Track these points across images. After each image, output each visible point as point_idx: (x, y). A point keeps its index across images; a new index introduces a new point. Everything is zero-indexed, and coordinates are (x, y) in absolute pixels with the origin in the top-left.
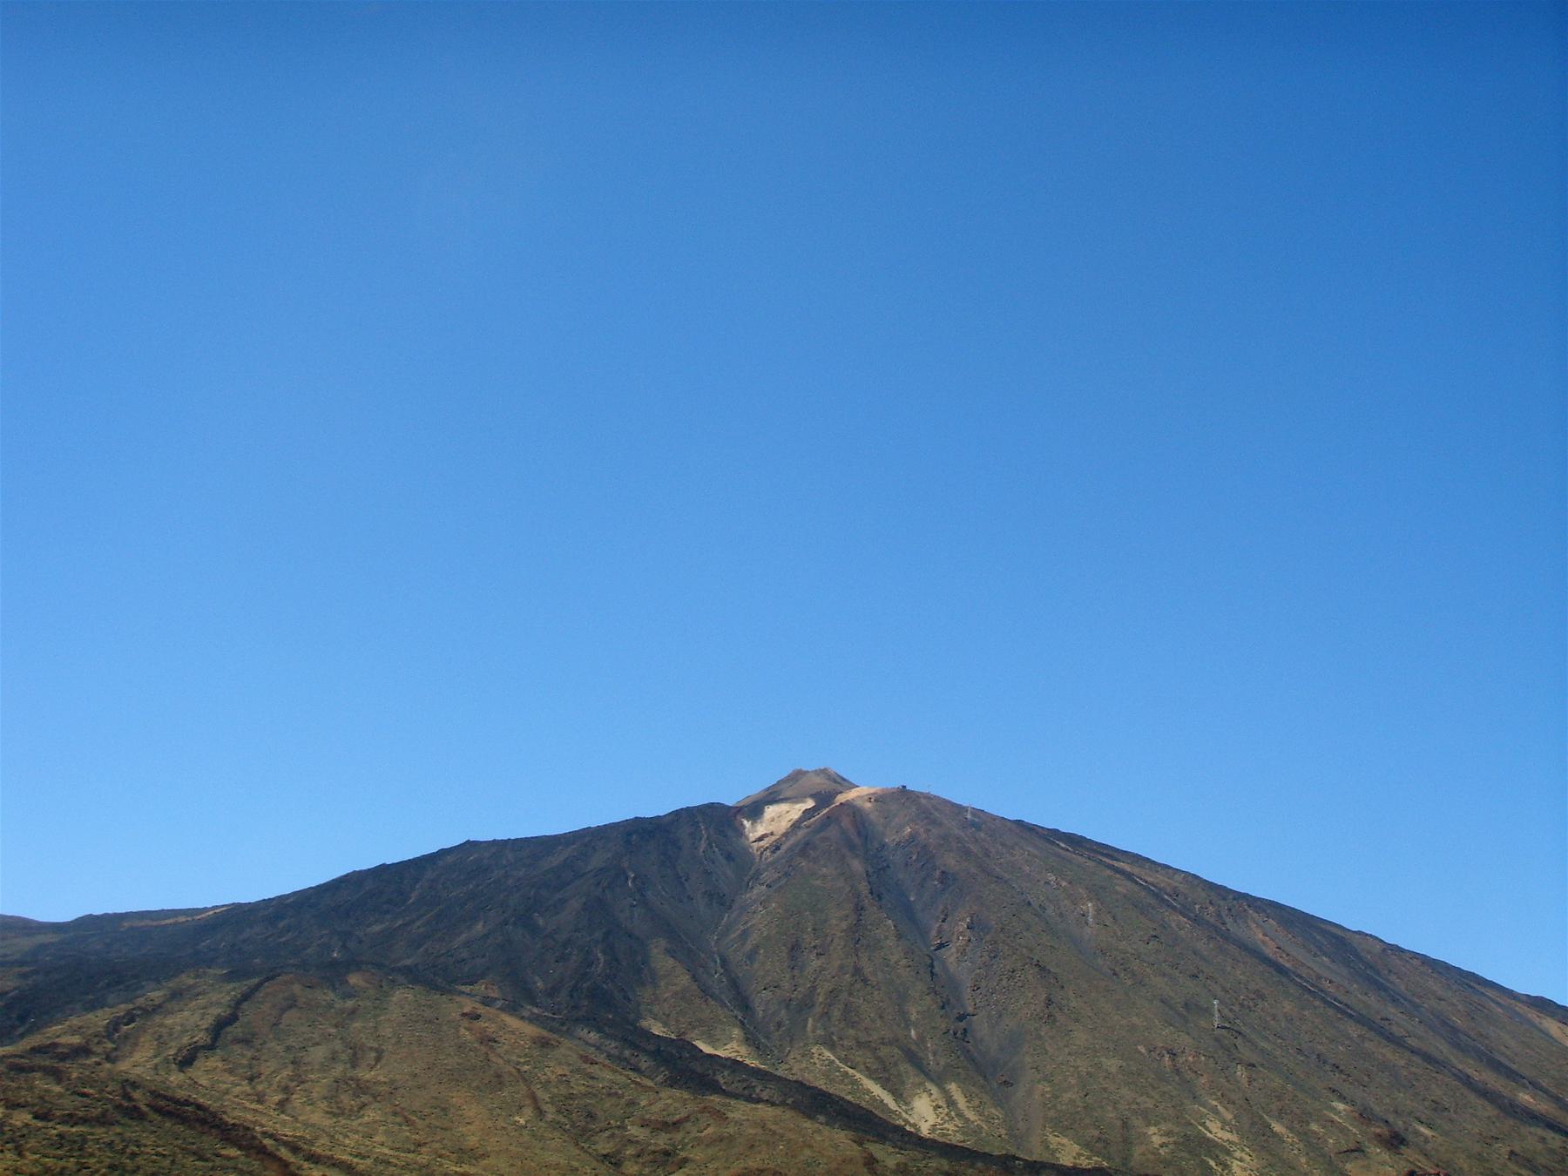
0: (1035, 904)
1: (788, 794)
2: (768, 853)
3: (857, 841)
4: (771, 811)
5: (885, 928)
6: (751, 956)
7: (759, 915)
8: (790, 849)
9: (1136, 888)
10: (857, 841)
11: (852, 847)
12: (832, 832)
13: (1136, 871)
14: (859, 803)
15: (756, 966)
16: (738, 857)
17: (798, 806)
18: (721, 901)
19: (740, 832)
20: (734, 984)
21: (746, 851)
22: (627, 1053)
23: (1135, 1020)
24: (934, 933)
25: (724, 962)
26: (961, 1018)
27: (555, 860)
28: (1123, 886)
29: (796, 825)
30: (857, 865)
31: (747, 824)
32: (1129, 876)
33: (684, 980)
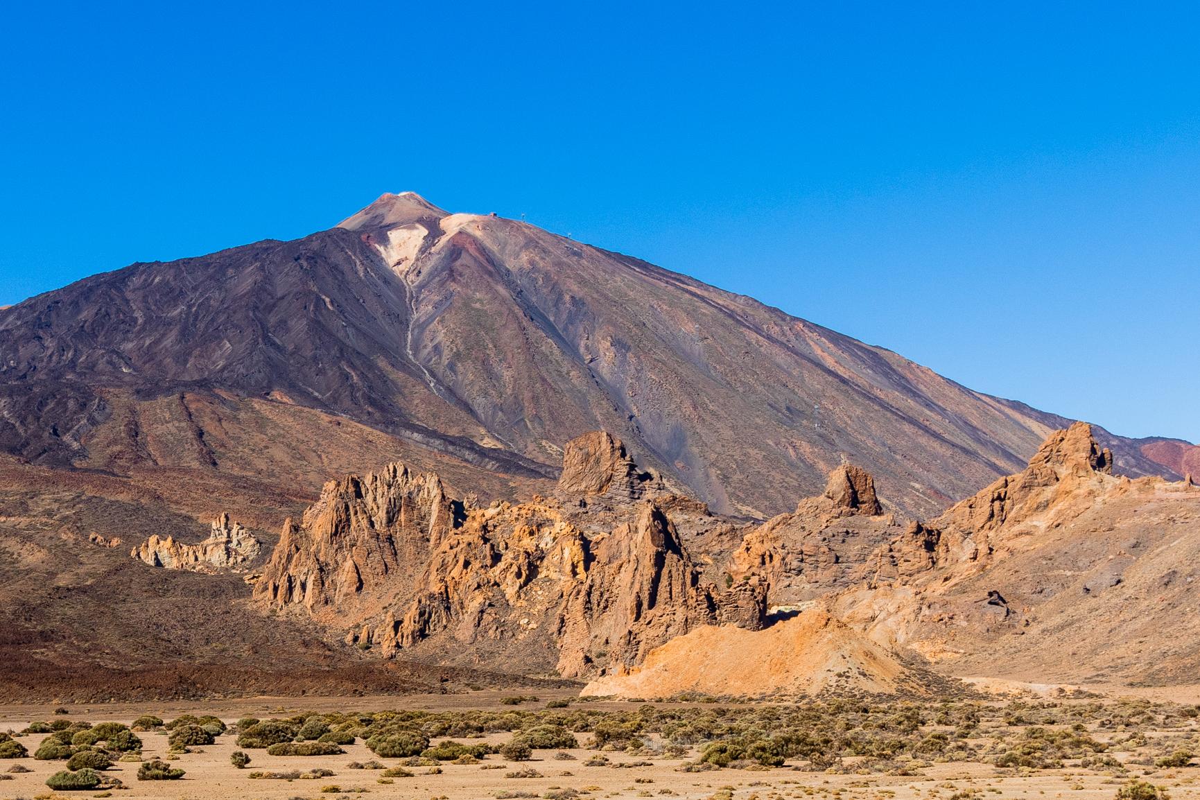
0: (649, 326)
1: (390, 219)
2: (411, 277)
3: (490, 268)
4: (393, 235)
5: (549, 346)
6: (452, 367)
7: (435, 332)
8: (432, 275)
9: (715, 311)
10: (490, 268)
11: (490, 274)
12: (464, 259)
13: (705, 294)
14: (470, 230)
15: (460, 378)
16: (388, 279)
17: (415, 232)
18: (400, 320)
19: (377, 254)
20: (450, 390)
21: (392, 274)
22: (451, 448)
23: (758, 421)
24: (582, 350)
25: (433, 374)
26: (631, 417)
27: (245, 281)
28: (705, 309)
29: (424, 250)
30: (501, 289)
31: (381, 249)
32: (702, 299)
33: (420, 389)
